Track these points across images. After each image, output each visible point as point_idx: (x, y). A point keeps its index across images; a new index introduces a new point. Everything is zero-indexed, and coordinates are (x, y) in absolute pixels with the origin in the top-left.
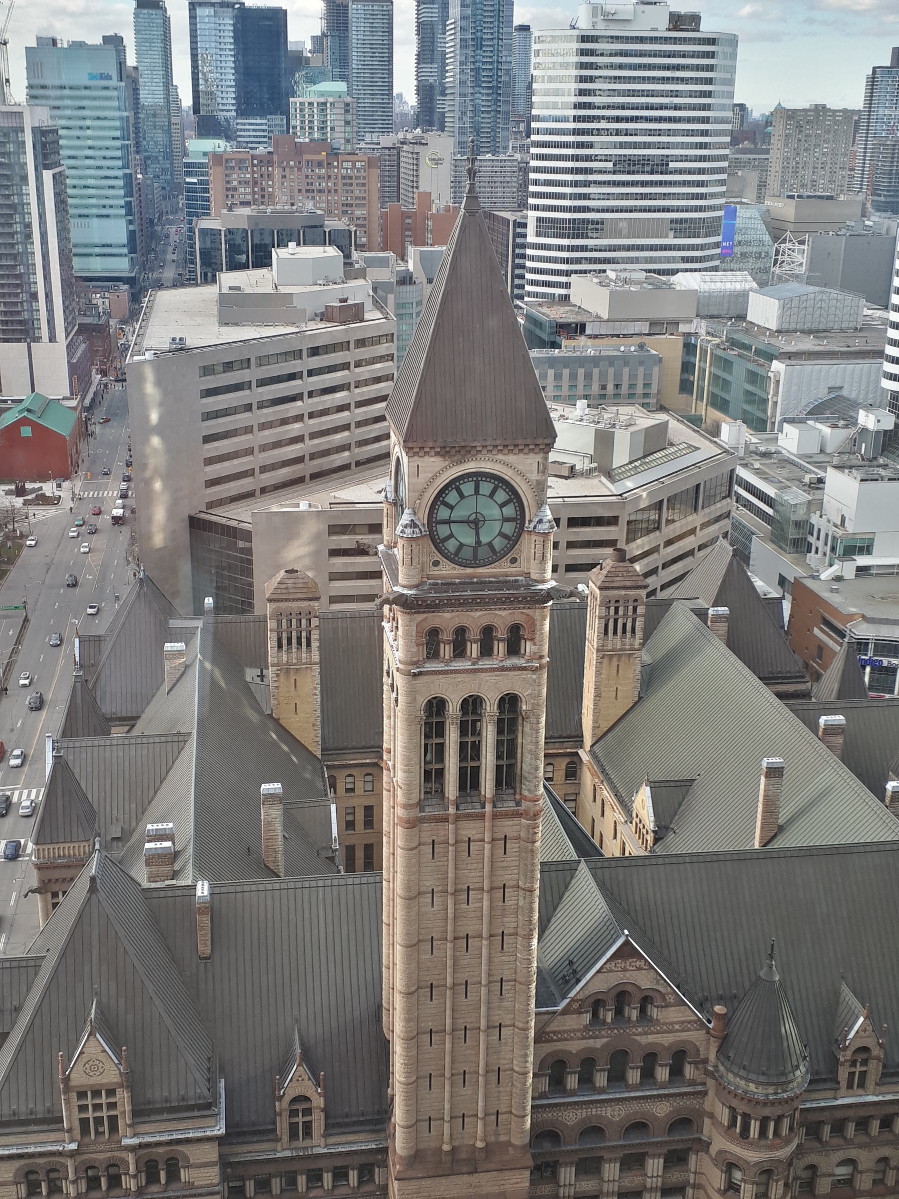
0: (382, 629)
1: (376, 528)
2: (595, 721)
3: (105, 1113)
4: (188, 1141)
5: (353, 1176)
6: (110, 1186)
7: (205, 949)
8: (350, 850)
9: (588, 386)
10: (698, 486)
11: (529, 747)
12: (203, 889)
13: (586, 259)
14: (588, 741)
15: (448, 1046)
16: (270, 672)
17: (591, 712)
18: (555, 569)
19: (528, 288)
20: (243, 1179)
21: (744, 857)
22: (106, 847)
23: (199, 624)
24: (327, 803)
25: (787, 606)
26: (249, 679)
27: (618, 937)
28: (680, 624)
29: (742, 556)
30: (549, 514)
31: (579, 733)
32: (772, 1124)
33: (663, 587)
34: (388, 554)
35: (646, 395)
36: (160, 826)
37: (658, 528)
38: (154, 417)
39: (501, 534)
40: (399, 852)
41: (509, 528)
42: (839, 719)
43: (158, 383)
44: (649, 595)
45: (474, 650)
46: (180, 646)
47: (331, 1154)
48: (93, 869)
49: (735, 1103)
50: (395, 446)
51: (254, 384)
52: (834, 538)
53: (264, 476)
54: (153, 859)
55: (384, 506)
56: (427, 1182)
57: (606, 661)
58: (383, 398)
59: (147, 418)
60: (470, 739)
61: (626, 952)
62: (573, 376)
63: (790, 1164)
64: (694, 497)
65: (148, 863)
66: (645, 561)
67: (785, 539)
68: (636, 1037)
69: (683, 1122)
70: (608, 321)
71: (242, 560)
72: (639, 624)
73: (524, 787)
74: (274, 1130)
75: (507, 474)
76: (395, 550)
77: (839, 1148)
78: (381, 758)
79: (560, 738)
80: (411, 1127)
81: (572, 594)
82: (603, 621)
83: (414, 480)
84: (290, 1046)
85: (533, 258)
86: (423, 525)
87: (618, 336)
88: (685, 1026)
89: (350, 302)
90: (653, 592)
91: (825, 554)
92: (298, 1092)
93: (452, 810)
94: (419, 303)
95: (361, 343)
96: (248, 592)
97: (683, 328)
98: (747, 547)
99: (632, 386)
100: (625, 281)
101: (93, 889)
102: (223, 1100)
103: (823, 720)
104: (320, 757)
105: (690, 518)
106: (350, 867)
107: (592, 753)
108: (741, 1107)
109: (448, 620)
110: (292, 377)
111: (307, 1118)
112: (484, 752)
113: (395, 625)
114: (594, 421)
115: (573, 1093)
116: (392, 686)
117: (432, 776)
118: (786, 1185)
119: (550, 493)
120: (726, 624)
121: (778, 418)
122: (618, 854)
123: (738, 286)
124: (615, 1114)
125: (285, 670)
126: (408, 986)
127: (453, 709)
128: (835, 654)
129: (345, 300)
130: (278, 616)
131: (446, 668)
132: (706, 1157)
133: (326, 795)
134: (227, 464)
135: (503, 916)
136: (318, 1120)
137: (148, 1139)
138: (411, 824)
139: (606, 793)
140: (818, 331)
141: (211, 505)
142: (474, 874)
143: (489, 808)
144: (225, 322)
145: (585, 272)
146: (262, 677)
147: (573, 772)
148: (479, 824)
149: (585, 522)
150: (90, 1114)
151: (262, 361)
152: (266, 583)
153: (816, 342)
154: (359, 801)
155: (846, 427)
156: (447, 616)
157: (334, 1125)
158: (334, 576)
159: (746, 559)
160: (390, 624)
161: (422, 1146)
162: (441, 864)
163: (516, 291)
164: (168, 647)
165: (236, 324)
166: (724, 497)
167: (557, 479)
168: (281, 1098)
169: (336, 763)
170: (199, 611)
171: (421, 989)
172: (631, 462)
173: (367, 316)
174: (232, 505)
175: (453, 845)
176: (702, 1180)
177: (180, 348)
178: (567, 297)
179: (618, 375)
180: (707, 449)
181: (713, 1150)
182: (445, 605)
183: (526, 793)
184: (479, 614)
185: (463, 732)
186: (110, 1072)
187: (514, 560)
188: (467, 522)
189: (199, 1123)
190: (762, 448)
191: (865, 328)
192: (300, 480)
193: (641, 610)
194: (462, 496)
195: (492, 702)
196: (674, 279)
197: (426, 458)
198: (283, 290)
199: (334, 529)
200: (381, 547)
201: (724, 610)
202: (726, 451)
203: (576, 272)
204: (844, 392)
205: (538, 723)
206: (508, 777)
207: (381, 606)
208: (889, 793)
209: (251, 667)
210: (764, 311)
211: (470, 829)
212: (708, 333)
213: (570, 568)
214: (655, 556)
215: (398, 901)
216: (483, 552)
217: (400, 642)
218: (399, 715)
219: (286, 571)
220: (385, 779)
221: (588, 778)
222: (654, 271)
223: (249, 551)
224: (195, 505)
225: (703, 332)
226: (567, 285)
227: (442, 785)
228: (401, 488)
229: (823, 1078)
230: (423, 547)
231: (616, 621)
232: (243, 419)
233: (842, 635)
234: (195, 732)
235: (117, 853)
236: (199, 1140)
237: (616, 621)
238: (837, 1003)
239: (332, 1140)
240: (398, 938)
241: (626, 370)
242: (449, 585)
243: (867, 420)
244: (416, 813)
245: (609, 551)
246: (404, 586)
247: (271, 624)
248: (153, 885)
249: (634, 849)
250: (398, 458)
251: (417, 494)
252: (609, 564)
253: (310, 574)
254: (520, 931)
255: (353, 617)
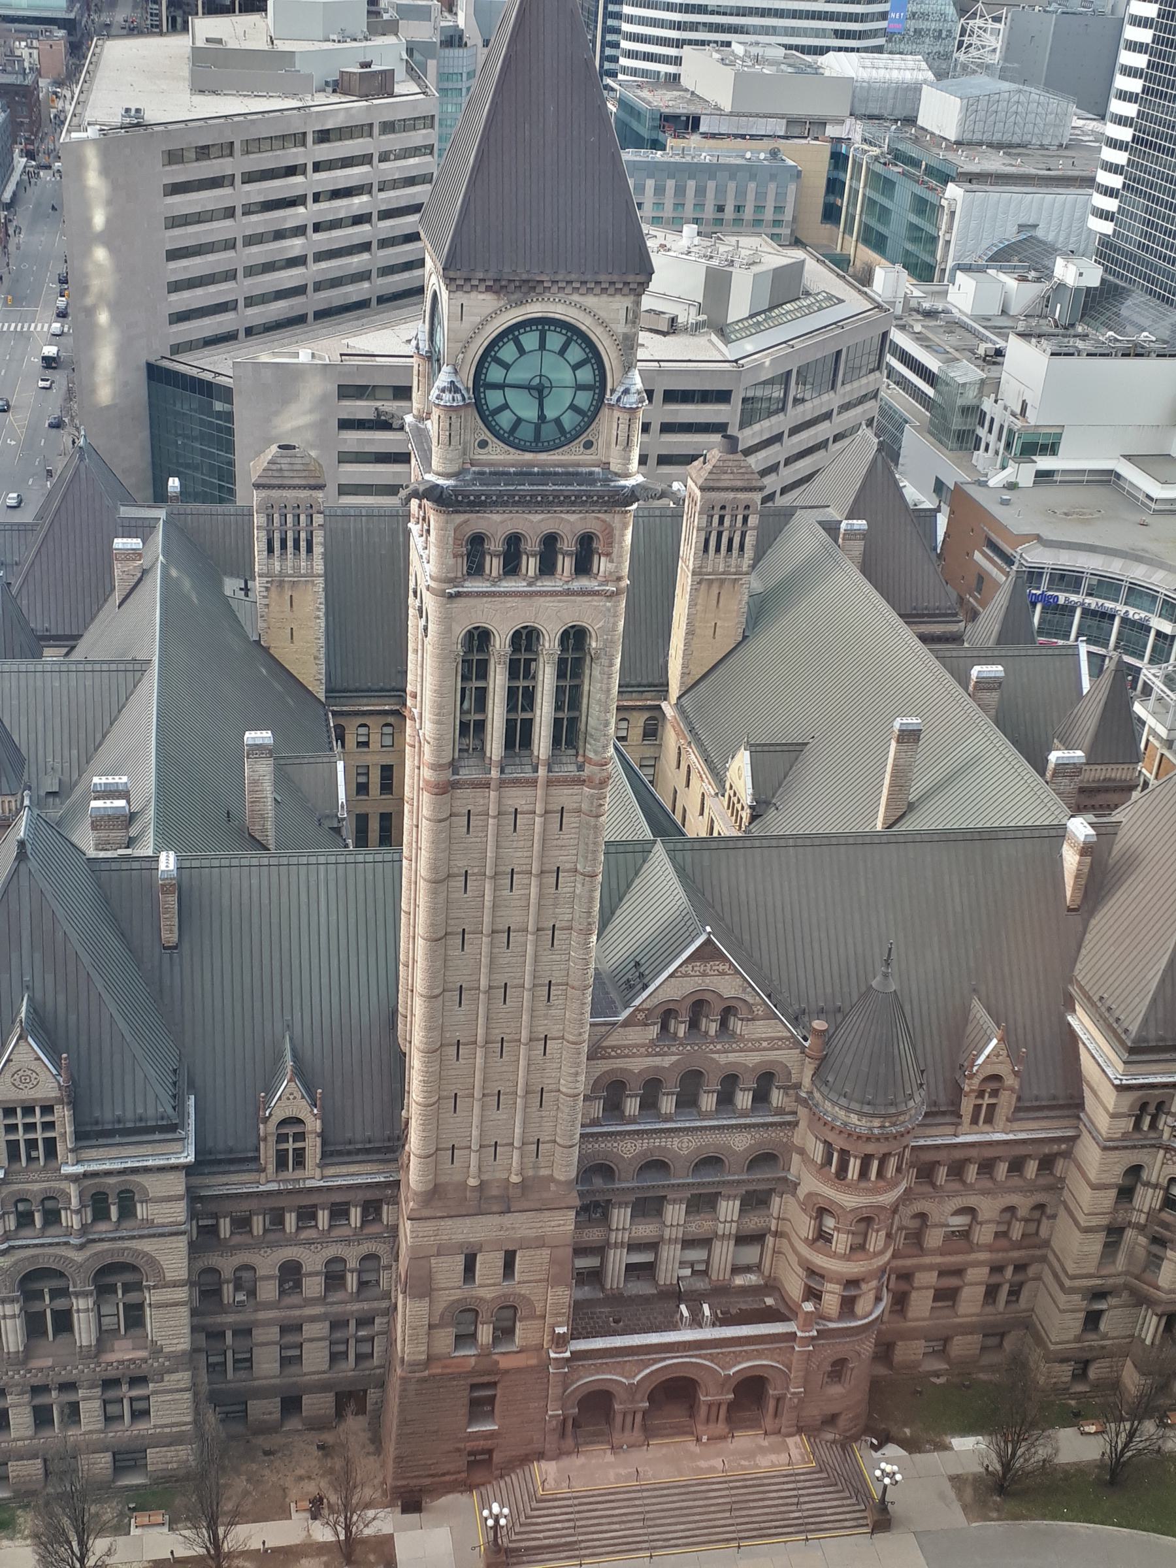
0: (408, 533)
1: (403, 393)
2: (685, 666)
3: (39, 1135)
4: (147, 1170)
5: (355, 1215)
6: (47, 1223)
7: (170, 936)
8: (362, 821)
9: (699, 206)
10: (839, 353)
11: (597, 695)
12: (167, 862)
13: (705, 24)
14: (674, 690)
15: (479, 1061)
16: (257, 585)
17: (681, 653)
18: (643, 460)
19: (624, 61)
20: (216, 1216)
21: (864, 841)
22: (38, 803)
23: (161, 513)
24: (333, 759)
25: (942, 521)
26: (228, 592)
27: (698, 935)
28: (803, 538)
29: (889, 452)
30: (637, 383)
31: (663, 680)
32: (876, 1163)
33: (784, 491)
34: (418, 428)
35: (777, 223)
36: (110, 780)
37: (783, 409)
38: (99, 219)
39: (573, 407)
40: (425, 824)
41: (584, 400)
42: (997, 670)
43: (105, 171)
44: (765, 500)
45: (531, 565)
46: (135, 543)
47: (329, 1188)
48: (21, 830)
49: (831, 1137)
50: (432, 278)
51: (238, 179)
52: (1010, 431)
53: (250, 311)
54: (101, 822)
55: (414, 361)
56: (449, 1222)
57: (704, 586)
58: (416, 208)
59: (88, 221)
60: (522, 683)
61: (707, 953)
62: (680, 191)
63: (895, 1211)
64: (830, 368)
65: (94, 827)
66: (762, 454)
67: (947, 430)
68: (715, 1056)
69: (765, 1159)
70: (731, 114)
71: (219, 429)
72: (750, 540)
73: (588, 746)
74: (257, 1159)
75: (585, 323)
76: (428, 423)
77: (956, 1194)
78: (405, 705)
79: (639, 686)
80: (431, 1157)
81: (663, 495)
82: (703, 534)
83: (456, 324)
84: (279, 1057)
85: (630, 19)
86: (467, 389)
87: (743, 137)
88: (775, 1043)
89: (374, 68)
90: (770, 497)
91: (997, 453)
92: (288, 1113)
93: (495, 773)
94: (471, 75)
95: (388, 127)
96: (227, 474)
97: (831, 131)
98: (897, 440)
99: (759, 208)
100: (757, 59)
101: (22, 856)
102: (192, 1121)
103: (975, 671)
104: (322, 696)
105: (825, 397)
106: (362, 840)
107: (678, 706)
108: (839, 1143)
109: (497, 524)
110: (291, 171)
111: (299, 1145)
112: (539, 701)
113: (426, 527)
114: (705, 256)
115: (633, 1120)
116: (420, 610)
117: (471, 730)
118: (889, 1236)
119: (641, 354)
120: (862, 543)
121: (950, 264)
122: (703, 834)
123: (908, 76)
124: (683, 1147)
125: (278, 582)
126: (430, 988)
127: (501, 644)
128: (997, 585)
129: (368, 65)
130: (268, 509)
131: (493, 589)
132: (791, 1200)
133: (331, 749)
134: (199, 291)
135: (555, 905)
136: (313, 1148)
137: (94, 1167)
138: (444, 789)
139: (693, 758)
140: (1010, 146)
141: (177, 349)
142: (520, 854)
143: (542, 771)
144: (199, 89)
145: (703, 43)
146: (246, 590)
147: (652, 732)
148: (529, 792)
149: (685, 397)
150: (20, 1136)
151: (253, 145)
152: (252, 463)
153: (1008, 160)
154: (375, 759)
155: (1038, 280)
156: (496, 517)
157: (332, 1154)
158: (346, 458)
159: (895, 456)
160: (419, 526)
161: (443, 1179)
162: (478, 840)
163: (607, 65)
164: (119, 543)
165: (214, 92)
166: (872, 371)
167: (653, 335)
168: (266, 1120)
169: (345, 709)
170: (160, 496)
171: (446, 992)
172: (751, 316)
173: (398, 89)
174: (207, 351)
175: (494, 817)
176: (787, 1228)
177: (135, 123)
178: (676, 78)
179: (741, 193)
180: (854, 303)
181: (802, 1192)
182: (495, 503)
183: (591, 755)
184: (539, 517)
185: (513, 673)
186: (46, 1083)
187: (588, 445)
188: (528, 388)
189: (160, 1148)
190: (926, 305)
191: (1073, 145)
192: (300, 320)
193: (753, 520)
194: (521, 351)
195: (552, 636)
196: (821, 60)
197: (474, 295)
198: (281, 46)
199: (347, 392)
200: (409, 419)
201: (860, 524)
202: (879, 306)
203: (690, 42)
204: (1040, 233)
205: (611, 665)
206: (567, 733)
207: (408, 500)
208: (1051, 766)
209: (232, 575)
210: (941, 113)
211: (517, 798)
212: (865, 140)
213: (663, 460)
214: (776, 447)
215: (422, 885)
216: (548, 431)
217: (433, 550)
218: (429, 648)
219: (280, 447)
220: (408, 731)
221: (671, 738)
222: (797, 48)
223: (229, 416)
224: (156, 350)
225: (857, 138)
226: (677, 61)
227: (483, 742)
228: (438, 337)
229: (945, 1110)
230: (466, 421)
231: (720, 534)
232: (221, 229)
233: (1009, 561)
234: (156, 659)
235: (54, 812)
236: (161, 1169)
237: (720, 534)
238: (966, 1021)
239: (330, 1171)
240: (421, 930)
241: (752, 186)
242: (499, 475)
243: (1066, 272)
244: (448, 775)
245: (716, 438)
246: (438, 474)
247: (258, 520)
248: (102, 854)
249: (725, 828)
250: (435, 293)
251: (461, 345)
252: (714, 456)
253: (313, 453)
254: (575, 925)
255: (371, 514)
